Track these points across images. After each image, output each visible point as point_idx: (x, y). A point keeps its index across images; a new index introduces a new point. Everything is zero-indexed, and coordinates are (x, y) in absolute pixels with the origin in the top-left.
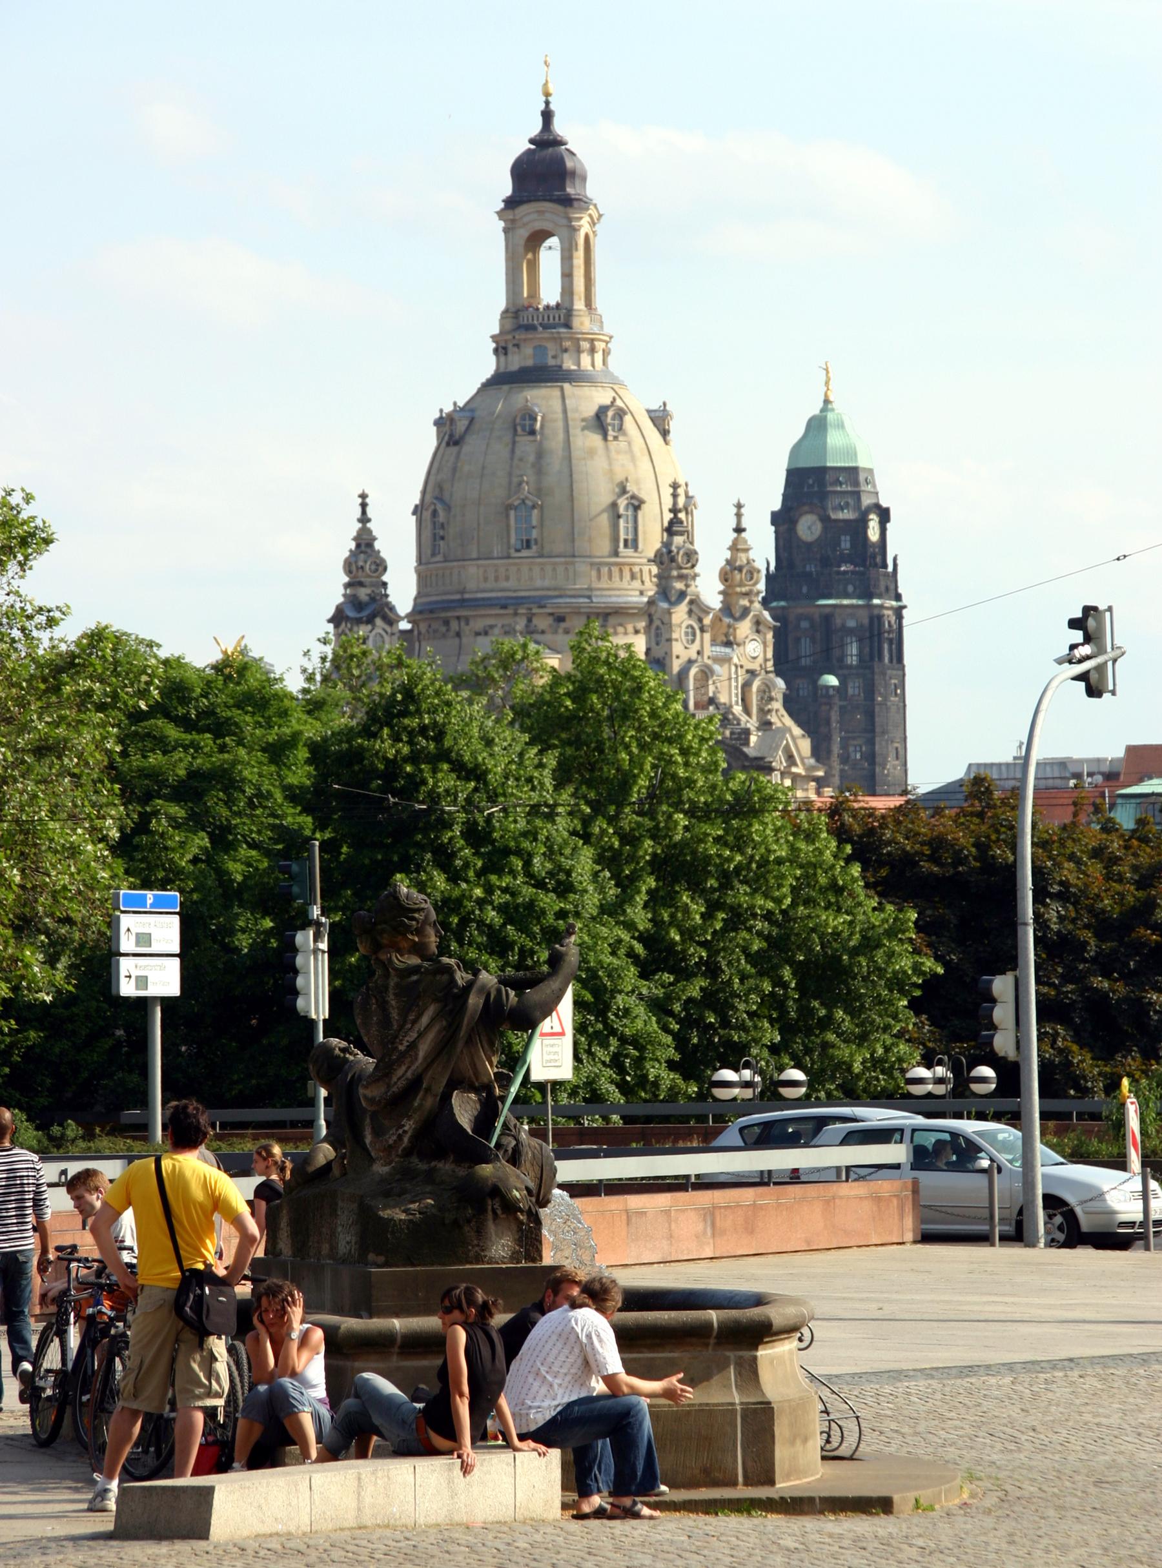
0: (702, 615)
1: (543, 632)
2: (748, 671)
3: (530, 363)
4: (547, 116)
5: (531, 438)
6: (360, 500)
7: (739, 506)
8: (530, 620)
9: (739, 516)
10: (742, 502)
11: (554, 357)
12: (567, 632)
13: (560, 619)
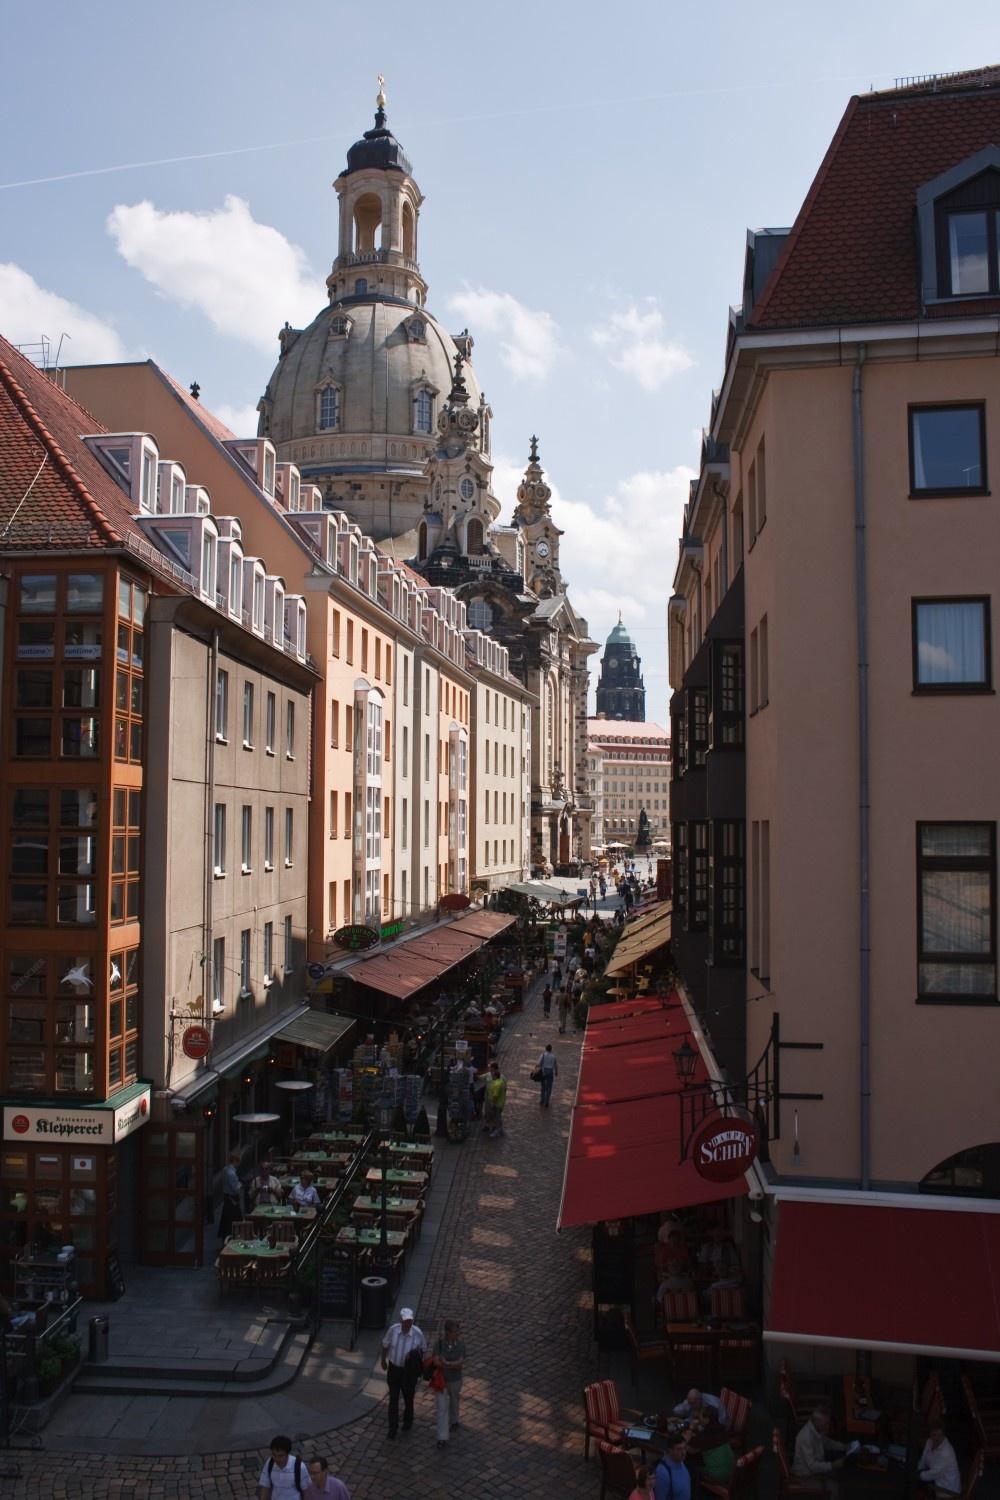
0: (481, 473)
1: (341, 499)
2: (538, 567)
3: (352, 293)
4: (380, 118)
5: (341, 337)
6: (191, 391)
7: (534, 440)
8: (330, 489)
9: (534, 447)
10: (536, 437)
11: (371, 287)
12: (362, 498)
13: (358, 487)
